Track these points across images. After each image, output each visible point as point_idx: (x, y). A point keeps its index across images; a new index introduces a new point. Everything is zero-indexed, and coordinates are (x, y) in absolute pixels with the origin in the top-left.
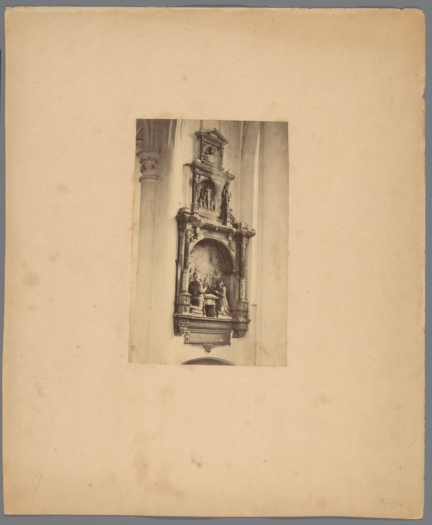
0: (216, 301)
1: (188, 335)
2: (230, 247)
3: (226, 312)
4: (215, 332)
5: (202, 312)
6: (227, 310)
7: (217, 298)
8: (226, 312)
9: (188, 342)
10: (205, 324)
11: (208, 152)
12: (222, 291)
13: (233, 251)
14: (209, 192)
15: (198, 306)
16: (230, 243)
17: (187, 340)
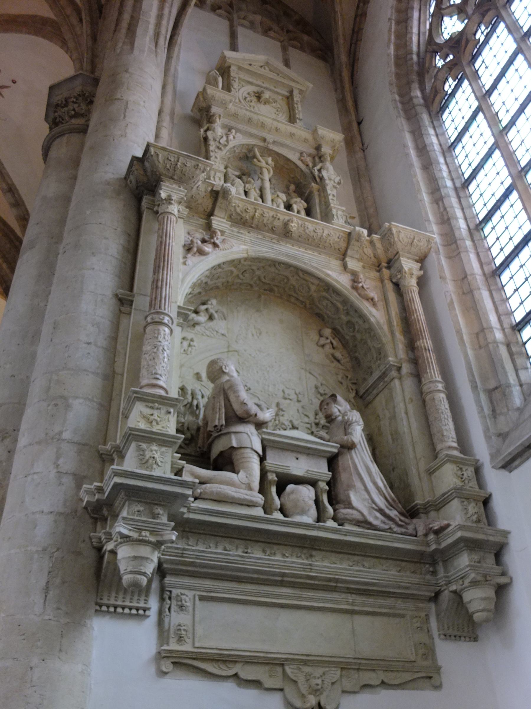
0: (332, 462)
1: (181, 607)
2: (355, 288)
3: (381, 511)
4: (342, 600)
5: (260, 499)
6: (381, 502)
7: (333, 448)
8: (381, 511)
9: (187, 647)
10: (278, 557)
12: (347, 426)
13: (374, 305)
14: (265, 171)
15: (238, 474)
16: (355, 280)
17: (180, 639)
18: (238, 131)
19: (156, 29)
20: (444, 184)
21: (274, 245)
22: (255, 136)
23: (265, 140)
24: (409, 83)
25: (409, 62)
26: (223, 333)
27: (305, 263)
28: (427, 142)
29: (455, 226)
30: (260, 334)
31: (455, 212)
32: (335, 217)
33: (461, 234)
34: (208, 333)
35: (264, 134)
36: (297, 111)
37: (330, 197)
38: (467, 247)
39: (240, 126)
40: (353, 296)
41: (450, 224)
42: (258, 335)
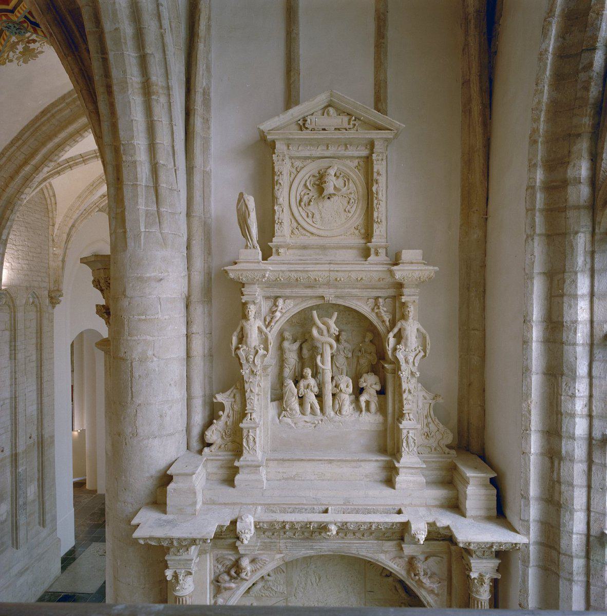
11: (313, 193)
18: (286, 298)
19: (151, 160)
20: (571, 432)
21: (314, 544)
22: (311, 298)
23: (323, 297)
24: (572, 136)
25: (583, 76)
26: (281, 591)
27: (352, 553)
28: (567, 318)
29: (565, 526)
30: (320, 579)
31: (572, 498)
32: (404, 444)
33: (569, 545)
34: (267, 593)
35: (320, 292)
36: (375, 202)
37: (405, 396)
38: (571, 574)
39: (288, 292)
40: (411, 584)
41: (558, 511)
42: (318, 580)
